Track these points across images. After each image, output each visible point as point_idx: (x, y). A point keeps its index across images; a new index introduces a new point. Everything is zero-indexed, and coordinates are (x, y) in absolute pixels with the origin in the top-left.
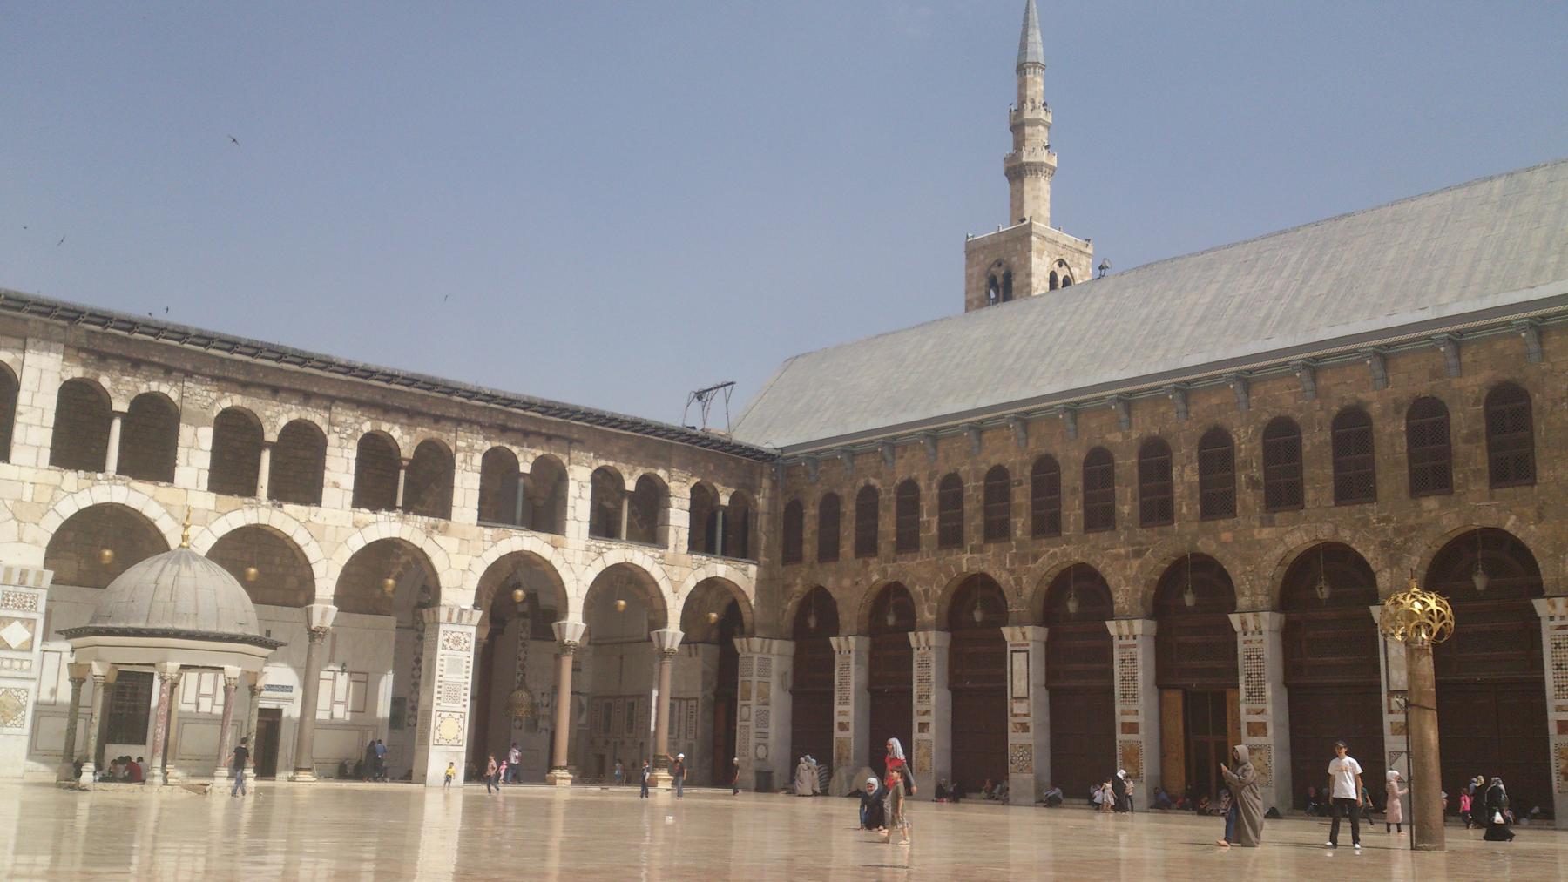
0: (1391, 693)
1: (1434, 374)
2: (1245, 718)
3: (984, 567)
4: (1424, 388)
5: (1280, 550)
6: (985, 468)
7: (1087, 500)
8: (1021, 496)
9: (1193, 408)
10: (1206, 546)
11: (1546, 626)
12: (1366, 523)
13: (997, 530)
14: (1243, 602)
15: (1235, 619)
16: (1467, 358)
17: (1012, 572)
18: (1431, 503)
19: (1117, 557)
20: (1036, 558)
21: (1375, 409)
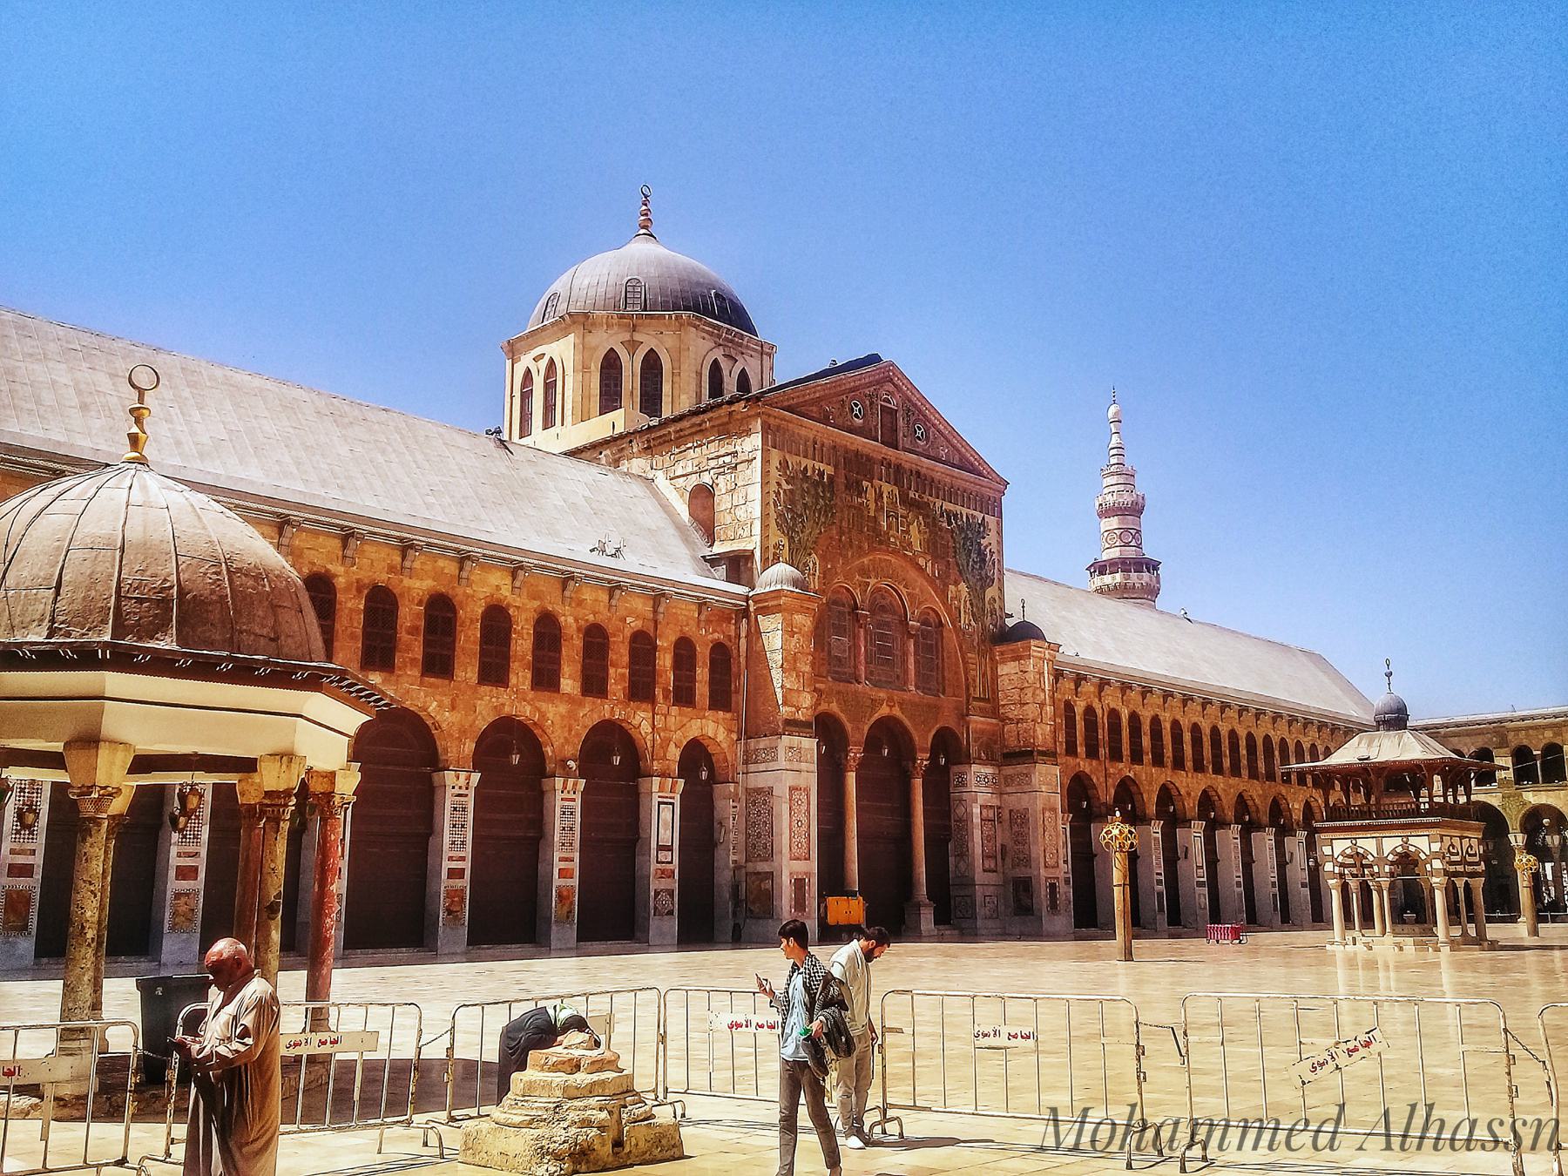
1: (391, 569)
2: (175, 861)
4: (382, 577)
11: (449, 792)
21: (340, 582)
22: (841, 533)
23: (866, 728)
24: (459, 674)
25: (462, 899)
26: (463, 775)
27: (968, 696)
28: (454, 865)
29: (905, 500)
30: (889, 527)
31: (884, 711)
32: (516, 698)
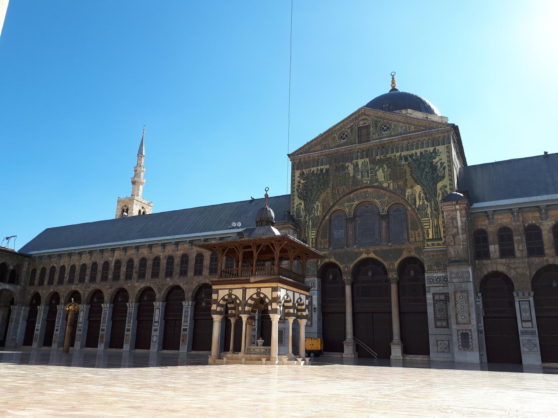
0: (155, 322)
1: (173, 251)
3: (77, 289)
4: (171, 253)
5: (139, 288)
6: (81, 264)
7: (102, 274)
8: (88, 272)
9: (127, 253)
10: (125, 287)
11: (184, 307)
12: (156, 283)
13: (82, 280)
14: (130, 300)
15: (128, 304)
16: (179, 248)
17: (83, 291)
18: (168, 279)
19: (107, 288)
20: (89, 288)
22: (333, 188)
23: (352, 266)
24: (189, 274)
25: (186, 337)
26: (187, 302)
27: (424, 238)
28: (184, 327)
29: (373, 162)
30: (362, 177)
31: (364, 256)
32: (176, 280)
